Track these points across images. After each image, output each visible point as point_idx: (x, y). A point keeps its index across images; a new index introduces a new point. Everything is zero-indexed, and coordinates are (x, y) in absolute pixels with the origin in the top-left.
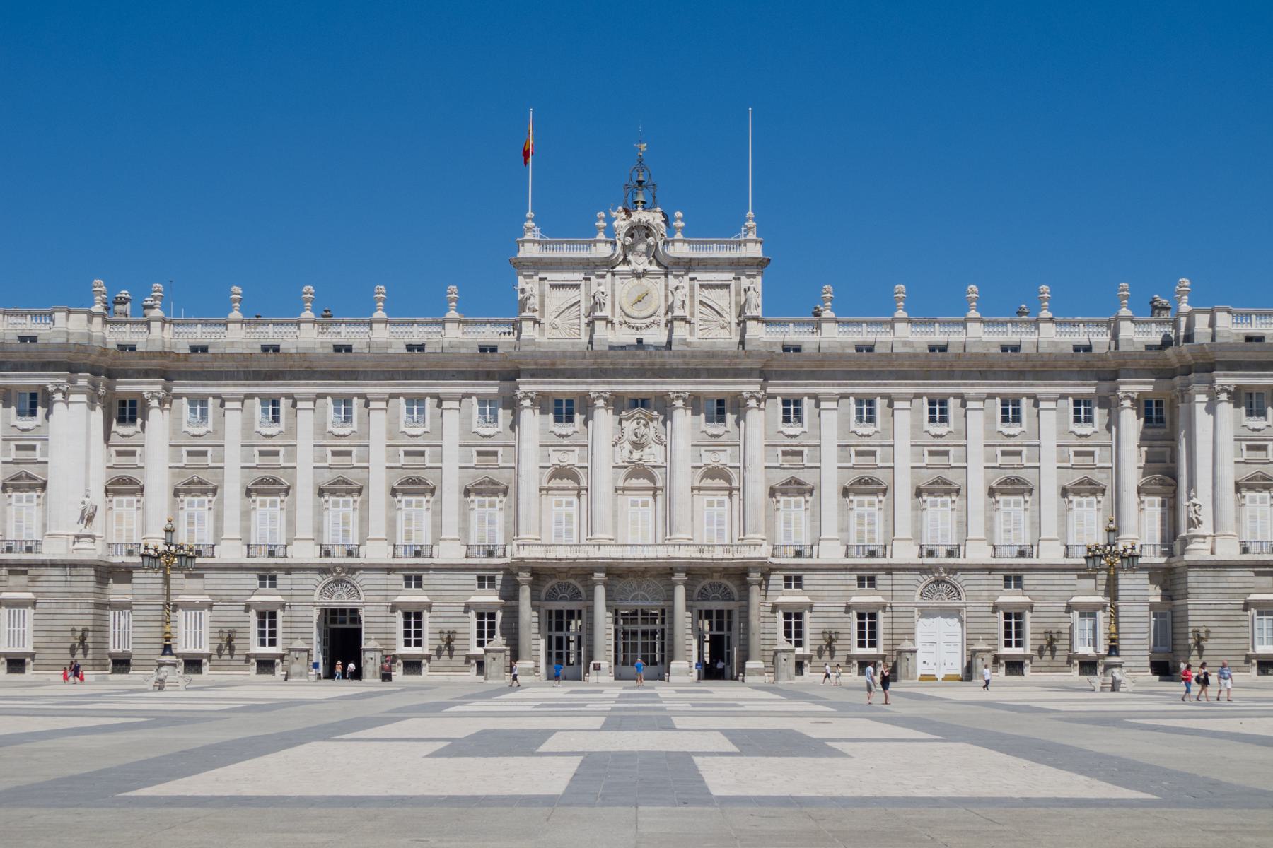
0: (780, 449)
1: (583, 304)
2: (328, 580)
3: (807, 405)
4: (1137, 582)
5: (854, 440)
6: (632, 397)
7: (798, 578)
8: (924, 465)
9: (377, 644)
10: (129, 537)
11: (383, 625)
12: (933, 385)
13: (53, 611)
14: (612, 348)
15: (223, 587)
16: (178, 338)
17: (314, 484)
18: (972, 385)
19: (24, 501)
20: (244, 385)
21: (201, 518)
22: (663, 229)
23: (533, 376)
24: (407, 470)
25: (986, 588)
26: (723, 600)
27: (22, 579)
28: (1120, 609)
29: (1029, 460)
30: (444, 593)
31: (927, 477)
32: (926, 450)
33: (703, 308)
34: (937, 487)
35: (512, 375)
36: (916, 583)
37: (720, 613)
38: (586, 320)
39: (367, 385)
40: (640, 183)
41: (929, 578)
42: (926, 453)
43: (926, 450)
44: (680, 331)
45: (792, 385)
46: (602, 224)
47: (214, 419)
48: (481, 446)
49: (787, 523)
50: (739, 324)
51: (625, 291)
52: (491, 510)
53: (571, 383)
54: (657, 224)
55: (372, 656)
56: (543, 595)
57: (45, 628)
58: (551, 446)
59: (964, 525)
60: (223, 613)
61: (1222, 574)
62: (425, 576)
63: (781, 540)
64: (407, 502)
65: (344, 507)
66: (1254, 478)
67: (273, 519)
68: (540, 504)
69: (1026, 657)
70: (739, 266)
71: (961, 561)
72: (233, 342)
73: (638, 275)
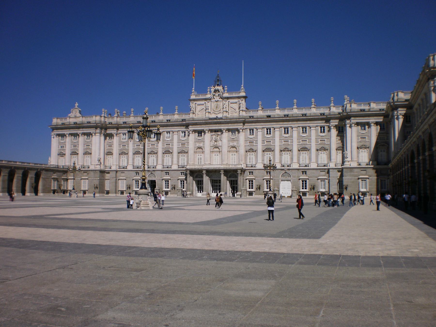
0: (248, 141)
1: (204, 109)
2: (149, 174)
3: (255, 130)
4: (334, 173)
7: (252, 172)
8: (282, 144)
10: (110, 164)
14: (210, 119)
16: (120, 120)
21: (124, 160)
22: (222, 90)
25: (297, 174)
26: (235, 178)
27: (86, 174)
28: (330, 180)
29: (308, 143)
31: (284, 147)
33: (231, 109)
34: (285, 150)
35: (187, 126)
37: (234, 181)
40: (218, 80)
41: (283, 172)
42: (283, 141)
43: (283, 141)
44: (225, 114)
46: (209, 90)
49: (250, 159)
51: (214, 106)
52: (184, 157)
54: (221, 89)
56: (195, 176)
59: (292, 159)
61: (352, 171)
63: (248, 163)
66: (362, 146)
67: (139, 160)
68: (194, 155)
69: (306, 192)
70: (239, 98)
71: (290, 168)
73: (216, 101)
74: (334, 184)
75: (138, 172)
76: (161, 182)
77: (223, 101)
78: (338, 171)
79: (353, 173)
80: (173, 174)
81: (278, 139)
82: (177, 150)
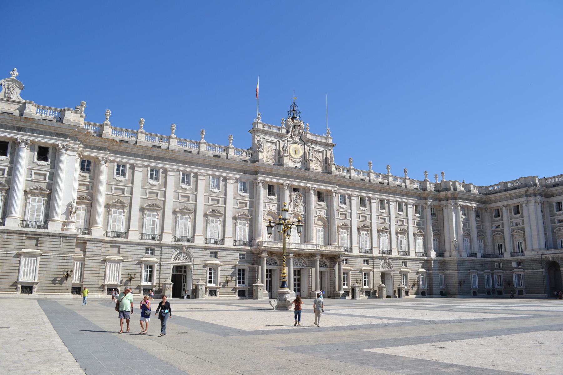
5: (360, 212)
6: (295, 187)
9: (203, 282)
11: (201, 273)
12: (381, 195)
13: (51, 260)
15: (129, 253)
17: (173, 209)
18: (392, 197)
19: (37, 201)
20: (145, 161)
21: (119, 219)
23: (263, 174)
24: (212, 207)
30: (226, 260)
32: (380, 217)
36: (380, 263)
38: (278, 156)
39: (198, 169)
40: (294, 110)
41: (383, 262)
45: (344, 190)
47: (128, 174)
48: (241, 200)
49: (342, 239)
50: (326, 166)
53: (277, 179)
55: (202, 287)
57: (45, 269)
58: (267, 203)
60: (129, 265)
61: (464, 263)
62: (219, 253)
64: (211, 220)
65: (185, 220)
67: (154, 222)
72: (141, 142)
73: (295, 143)
74: (436, 279)
75: (153, 247)
76: (201, 271)
77: (304, 145)
78: (439, 262)
79: (464, 267)
80: (226, 255)
81: (376, 214)
82: (233, 212)
